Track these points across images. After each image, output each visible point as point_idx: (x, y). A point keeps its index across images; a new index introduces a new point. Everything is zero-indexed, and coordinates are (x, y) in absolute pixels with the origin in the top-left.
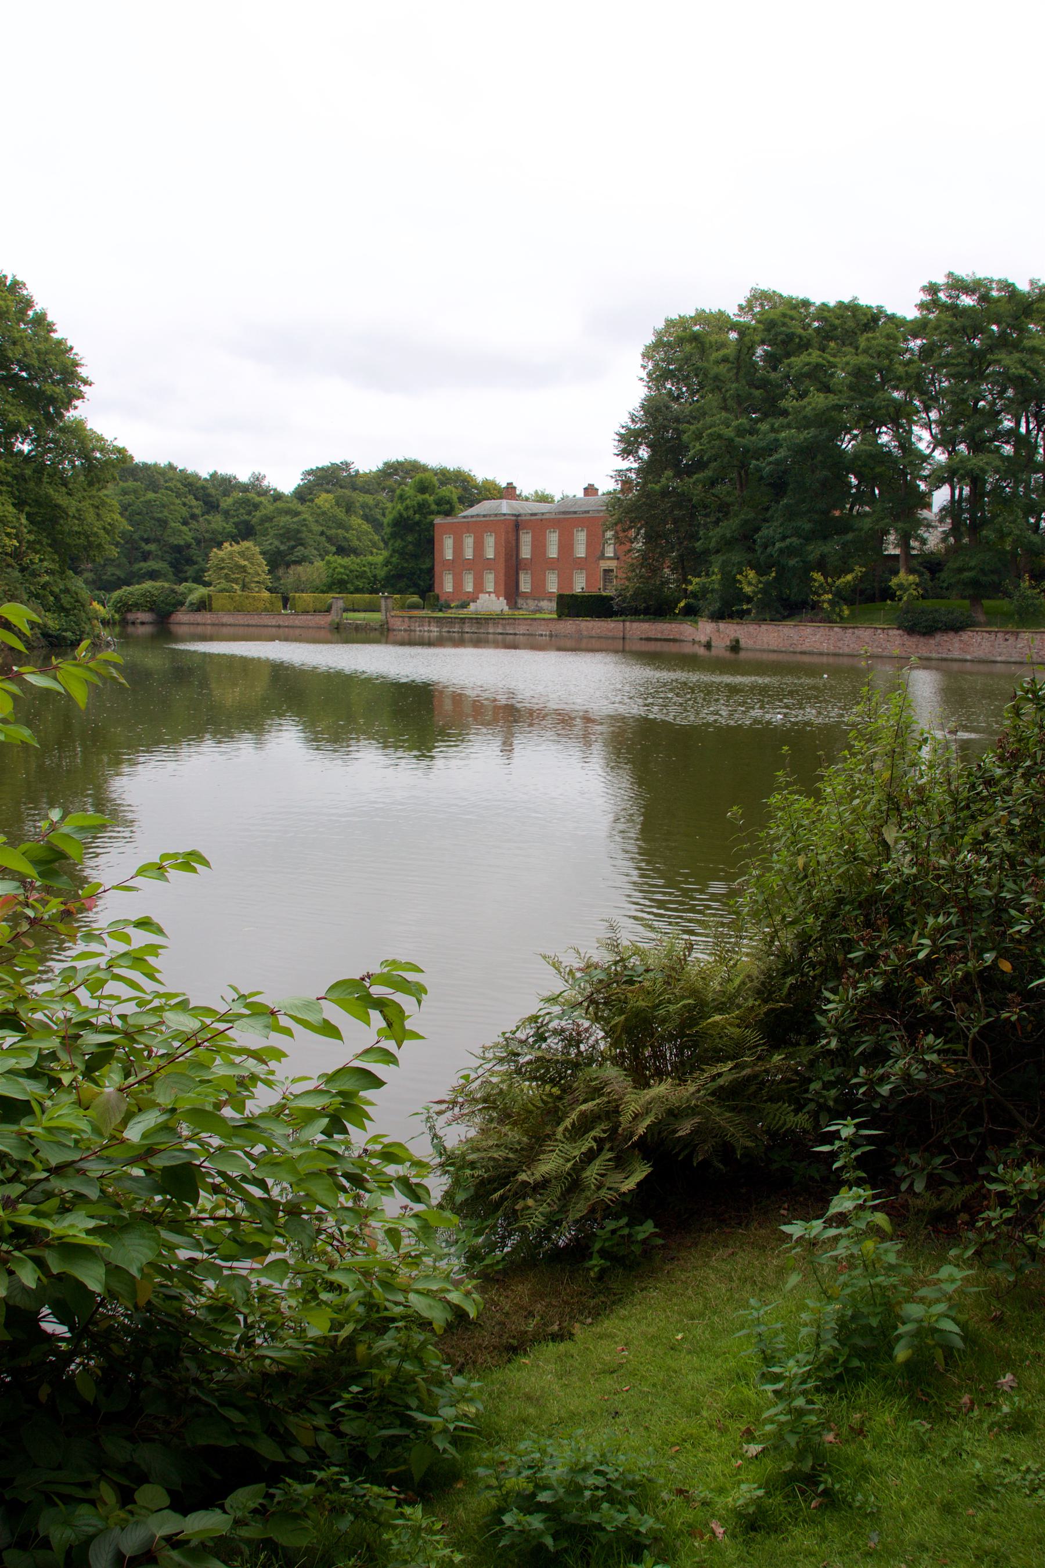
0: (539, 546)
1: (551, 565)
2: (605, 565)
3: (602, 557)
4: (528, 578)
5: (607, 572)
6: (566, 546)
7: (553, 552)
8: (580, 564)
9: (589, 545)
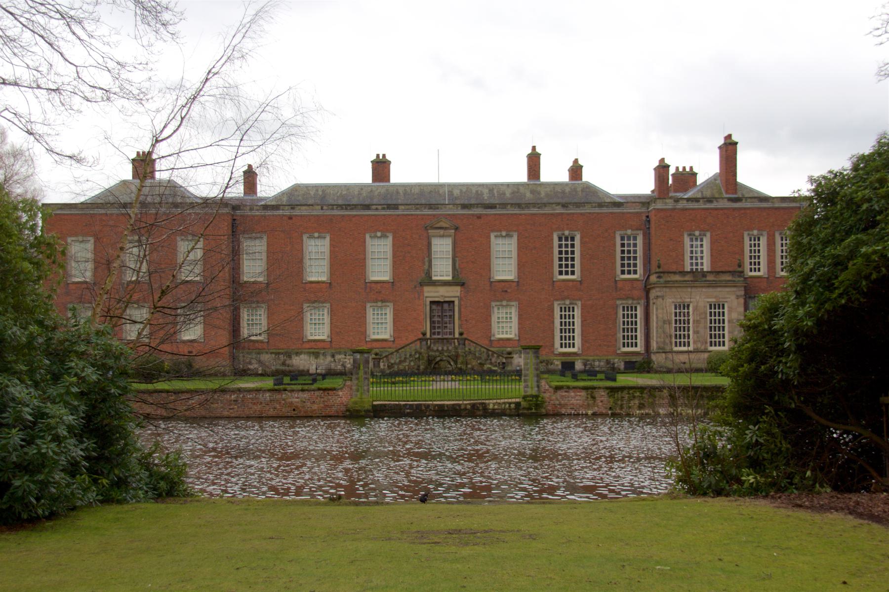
0: (286, 262)
1: (317, 294)
2: (432, 293)
8: (379, 293)
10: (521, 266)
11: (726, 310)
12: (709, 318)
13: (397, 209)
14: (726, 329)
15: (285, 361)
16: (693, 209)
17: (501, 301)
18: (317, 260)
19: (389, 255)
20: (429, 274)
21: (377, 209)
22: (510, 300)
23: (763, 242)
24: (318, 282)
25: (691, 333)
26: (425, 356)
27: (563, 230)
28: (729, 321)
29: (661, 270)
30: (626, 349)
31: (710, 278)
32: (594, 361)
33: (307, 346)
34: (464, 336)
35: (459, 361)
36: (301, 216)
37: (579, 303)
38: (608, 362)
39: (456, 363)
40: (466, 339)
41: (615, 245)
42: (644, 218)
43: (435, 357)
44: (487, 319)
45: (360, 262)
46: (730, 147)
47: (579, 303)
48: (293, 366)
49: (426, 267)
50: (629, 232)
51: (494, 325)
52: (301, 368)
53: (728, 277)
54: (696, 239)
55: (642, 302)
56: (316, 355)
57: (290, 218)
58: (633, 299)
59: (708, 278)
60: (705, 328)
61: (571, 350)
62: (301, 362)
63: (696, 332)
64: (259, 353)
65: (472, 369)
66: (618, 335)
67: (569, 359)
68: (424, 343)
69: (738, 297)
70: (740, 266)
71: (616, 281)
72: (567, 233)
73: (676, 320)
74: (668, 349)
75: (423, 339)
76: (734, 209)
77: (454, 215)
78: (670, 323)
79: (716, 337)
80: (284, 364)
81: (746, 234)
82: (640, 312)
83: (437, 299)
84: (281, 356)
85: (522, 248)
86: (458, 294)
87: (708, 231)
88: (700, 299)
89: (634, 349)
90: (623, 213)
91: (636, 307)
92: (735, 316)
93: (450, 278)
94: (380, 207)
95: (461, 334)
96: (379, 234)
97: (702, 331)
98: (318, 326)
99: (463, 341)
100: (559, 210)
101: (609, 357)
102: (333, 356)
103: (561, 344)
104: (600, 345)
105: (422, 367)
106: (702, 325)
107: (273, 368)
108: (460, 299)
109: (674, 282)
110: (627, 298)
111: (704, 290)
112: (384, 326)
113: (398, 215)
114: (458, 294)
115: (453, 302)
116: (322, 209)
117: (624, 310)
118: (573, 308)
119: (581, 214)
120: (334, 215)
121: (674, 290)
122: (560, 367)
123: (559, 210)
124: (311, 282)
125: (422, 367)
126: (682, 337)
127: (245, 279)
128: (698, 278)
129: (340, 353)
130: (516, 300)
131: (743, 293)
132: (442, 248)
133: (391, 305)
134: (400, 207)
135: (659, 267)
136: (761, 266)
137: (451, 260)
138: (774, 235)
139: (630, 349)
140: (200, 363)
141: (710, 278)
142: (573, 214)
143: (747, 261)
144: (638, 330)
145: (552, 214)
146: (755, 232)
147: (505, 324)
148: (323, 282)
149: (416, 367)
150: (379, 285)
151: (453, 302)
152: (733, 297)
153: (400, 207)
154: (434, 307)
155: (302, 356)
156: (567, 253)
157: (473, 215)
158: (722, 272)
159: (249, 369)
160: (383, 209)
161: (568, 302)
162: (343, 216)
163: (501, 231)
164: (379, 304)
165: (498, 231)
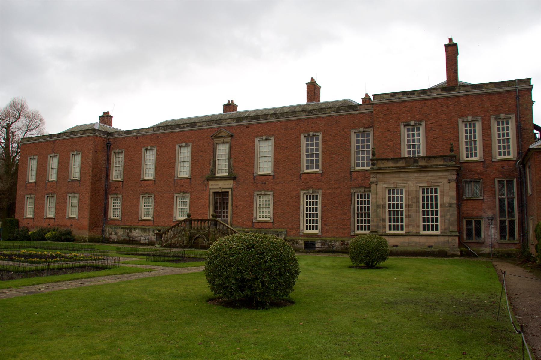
0: (133, 167)
1: (147, 188)
2: (216, 186)
3: (213, 177)
5: (221, 196)
6: (166, 165)
7: (149, 173)
8: (182, 186)
9: (194, 162)
10: (276, 163)
11: (438, 195)
12: (421, 202)
15: (128, 233)
16: (408, 101)
22: (267, 190)
23: (478, 127)
27: (309, 132)
28: (441, 205)
32: (331, 241)
33: (141, 224)
35: (210, 238)
37: (320, 192)
38: (343, 243)
41: (350, 142)
43: (194, 235)
44: (250, 206)
47: (320, 192)
49: (211, 166)
56: (144, 230)
57: (137, 138)
59: (420, 164)
62: (136, 234)
64: (116, 228)
66: (353, 219)
69: (449, 181)
70: (451, 151)
71: (351, 172)
73: (390, 205)
76: (448, 98)
77: (231, 126)
78: (384, 207)
80: (128, 235)
83: (217, 191)
84: (127, 230)
85: (277, 148)
86: (231, 186)
87: (423, 120)
88: (412, 184)
90: (357, 114)
92: (446, 200)
93: (227, 174)
94: (185, 125)
97: (413, 215)
100: (305, 116)
101: (344, 239)
103: (307, 226)
104: (337, 228)
106: (414, 209)
107: (122, 238)
109: (386, 168)
110: (360, 187)
111: (416, 175)
113: (196, 130)
114: (231, 186)
115: (228, 192)
117: (358, 198)
118: (317, 196)
119: (323, 117)
120: (159, 134)
122: (303, 246)
123: (305, 116)
124: (146, 180)
125: (185, 242)
126: (396, 222)
127: (114, 179)
128: (412, 164)
130: (271, 191)
131: (455, 177)
133: (188, 195)
134: (198, 124)
136: (478, 151)
137: (227, 160)
138: (489, 120)
140: (76, 233)
141: (422, 163)
142: (317, 118)
143: (463, 146)
145: (300, 120)
146: (470, 118)
148: (151, 180)
149: (182, 241)
150: (182, 181)
151: (228, 192)
152: (445, 181)
155: (137, 231)
156: (312, 150)
157: (243, 125)
159: (110, 238)
160: (188, 127)
161: (311, 191)
162: (164, 133)
163: (262, 136)
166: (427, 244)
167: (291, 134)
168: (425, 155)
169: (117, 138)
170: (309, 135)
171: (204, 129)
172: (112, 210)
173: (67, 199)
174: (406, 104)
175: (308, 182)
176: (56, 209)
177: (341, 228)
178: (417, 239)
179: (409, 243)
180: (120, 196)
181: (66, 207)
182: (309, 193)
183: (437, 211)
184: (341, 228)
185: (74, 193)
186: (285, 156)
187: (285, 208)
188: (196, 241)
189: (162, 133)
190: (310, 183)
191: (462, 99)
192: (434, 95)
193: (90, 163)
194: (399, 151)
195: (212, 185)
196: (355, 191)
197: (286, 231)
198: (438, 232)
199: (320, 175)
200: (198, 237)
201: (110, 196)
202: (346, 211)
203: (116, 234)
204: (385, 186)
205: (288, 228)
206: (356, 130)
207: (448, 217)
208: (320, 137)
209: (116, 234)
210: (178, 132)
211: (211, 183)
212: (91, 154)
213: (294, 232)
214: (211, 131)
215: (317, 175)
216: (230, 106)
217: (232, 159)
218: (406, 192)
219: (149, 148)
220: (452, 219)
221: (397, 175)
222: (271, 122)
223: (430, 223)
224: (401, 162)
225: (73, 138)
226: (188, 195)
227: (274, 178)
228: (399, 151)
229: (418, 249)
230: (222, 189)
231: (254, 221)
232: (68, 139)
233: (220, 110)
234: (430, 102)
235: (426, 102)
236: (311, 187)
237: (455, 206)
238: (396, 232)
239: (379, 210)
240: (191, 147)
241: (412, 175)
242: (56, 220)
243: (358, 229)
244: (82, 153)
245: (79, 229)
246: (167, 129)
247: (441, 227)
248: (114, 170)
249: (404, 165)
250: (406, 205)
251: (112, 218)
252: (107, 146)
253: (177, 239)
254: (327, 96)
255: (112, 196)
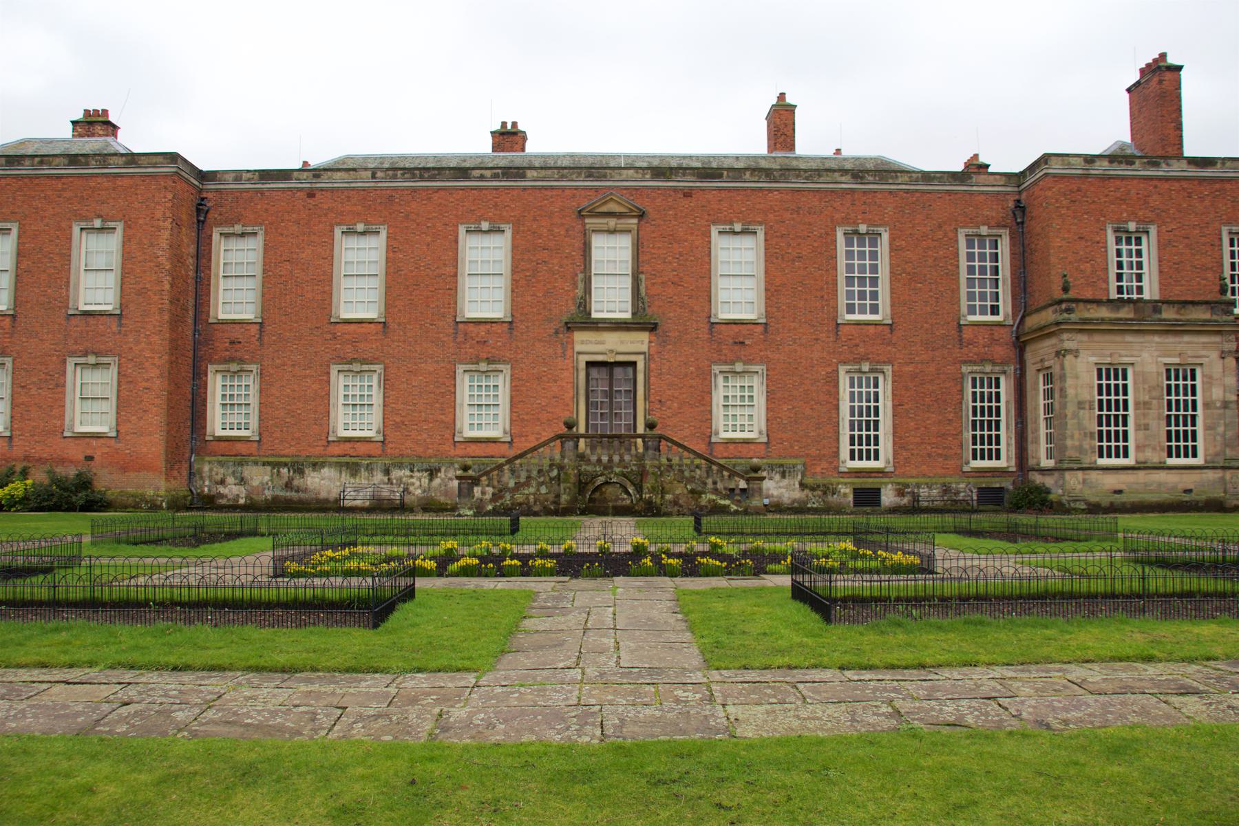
0: (298, 283)
1: (355, 345)
2: (588, 345)
4: (249, 387)
6: (422, 282)
8: (483, 344)
9: (524, 275)
10: (772, 292)
11: (1198, 382)
13: (523, 176)
14: (1199, 421)
15: (290, 480)
16: (1123, 178)
17: (733, 363)
18: (359, 279)
19: (505, 267)
20: (584, 305)
21: (482, 178)
24: (360, 322)
25: (1131, 428)
26: (572, 473)
28: (1207, 405)
29: (1071, 295)
30: (979, 464)
31: (1168, 314)
32: (918, 486)
34: (656, 431)
35: (647, 485)
36: (332, 190)
37: (888, 369)
38: (946, 490)
39: (639, 489)
40: (661, 437)
41: (956, 255)
42: (1011, 204)
45: (446, 282)
46: (1168, 76)
47: (888, 369)
48: (306, 490)
49: (579, 292)
50: (984, 230)
51: (718, 412)
52: (323, 495)
53: (1201, 314)
54: (1128, 242)
55: (1011, 369)
56: (354, 469)
57: (311, 194)
58: (994, 363)
59: (1164, 315)
60: (1159, 415)
61: (872, 464)
62: (323, 482)
63: (1142, 427)
64: (241, 464)
65: (675, 503)
66: (965, 434)
67: (869, 482)
68: (570, 444)
71: (960, 326)
72: (863, 228)
74: (1086, 461)
75: (568, 435)
76: (1202, 180)
77: (636, 189)
79: (1180, 439)
80: (288, 486)
81: (1225, 231)
82: (1006, 389)
85: (772, 257)
87: (1151, 222)
88: (1147, 358)
89: (993, 463)
90: (971, 193)
91: (997, 380)
92: (1217, 394)
94: (488, 173)
95: (650, 426)
96: (485, 226)
97: (1153, 424)
98: (356, 408)
99: (655, 440)
100: (847, 184)
101: (948, 480)
102: (387, 472)
103: (852, 452)
104: (929, 455)
105: (565, 498)
106: (1153, 413)
107: (268, 494)
108: (649, 358)
109: (1103, 321)
110: (982, 361)
111: (1157, 339)
112: (492, 411)
113: (525, 189)
114: (644, 348)
115: (634, 364)
116: (374, 176)
117: (974, 386)
119: (891, 192)
120: (396, 189)
121: (1097, 337)
122: (851, 498)
123: (847, 184)
125: (565, 498)
127: (221, 316)
128: (1142, 317)
129: (400, 466)
130: (761, 363)
132: (612, 255)
133: (506, 369)
134: (530, 174)
135: (1066, 289)
137: (629, 280)
139: (986, 464)
140: (107, 482)
141: (1168, 314)
144: (1003, 426)
145: (833, 191)
147: (739, 411)
148: (371, 322)
149: (551, 497)
150: (482, 328)
151: (634, 364)
152: (1214, 355)
153: (530, 174)
154: (594, 372)
155: (326, 471)
156: (862, 268)
157: (675, 189)
158: (1193, 303)
159: (222, 496)
162: (414, 190)
163: (731, 223)
164: (483, 366)
165: (725, 223)
166: (1181, 487)
167: (810, 224)
168: (1157, 297)
169: (232, 191)
170: (856, 232)
171: (552, 188)
172: (219, 410)
173: (64, 373)
174: (1118, 182)
175: (857, 345)
176: (14, 405)
177: (940, 455)
178: (1161, 476)
179: (1146, 485)
180: (254, 367)
181: (63, 399)
182: (860, 371)
183: (1125, 417)
184: (940, 455)
185: (97, 354)
186: (796, 276)
187: (800, 407)
188: (597, 495)
189: (407, 188)
190: (864, 347)
191: (1228, 186)
192: (1102, 167)
193: (163, 260)
194: (1104, 286)
195: (582, 342)
196: (970, 369)
197: (804, 465)
198: (1199, 461)
199: (887, 330)
200: (606, 483)
201: (211, 368)
202: (951, 416)
203: (242, 481)
204: (1094, 359)
205: (807, 455)
206: (970, 231)
207: (1221, 429)
208: (885, 237)
209: (242, 481)
210: (463, 189)
211: (579, 336)
212: (167, 234)
213: (824, 464)
214: (574, 196)
215: (880, 328)
216: (509, 137)
217: (643, 277)
218: (1135, 374)
219: (360, 227)
220: (1229, 434)
221: (1118, 338)
222: (753, 190)
223: (1180, 439)
224: (1126, 309)
225: (81, 176)
226: (506, 369)
227: (766, 331)
228: (1104, 286)
229: (1165, 497)
230: (618, 353)
231: (714, 439)
232: (59, 177)
233: (484, 146)
234: (1167, 185)
235: (1159, 184)
236: (864, 358)
237: (1234, 406)
238: (1182, 461)
239: (1082, 412)
240: (509, 234)
241: (1148, 338)
242: (16, 441)
243: (975, 458)
244: (127, 227)
245: (124, 469)
246: (422, 178)
247: (1206, 450)
248: (221, 287)
249: (1131, 316)
250: (1137, 404)
251: (220, 433)
252: (199, 211)
253: (532, 490)
254: (811, 142)
255: (221, 367)
